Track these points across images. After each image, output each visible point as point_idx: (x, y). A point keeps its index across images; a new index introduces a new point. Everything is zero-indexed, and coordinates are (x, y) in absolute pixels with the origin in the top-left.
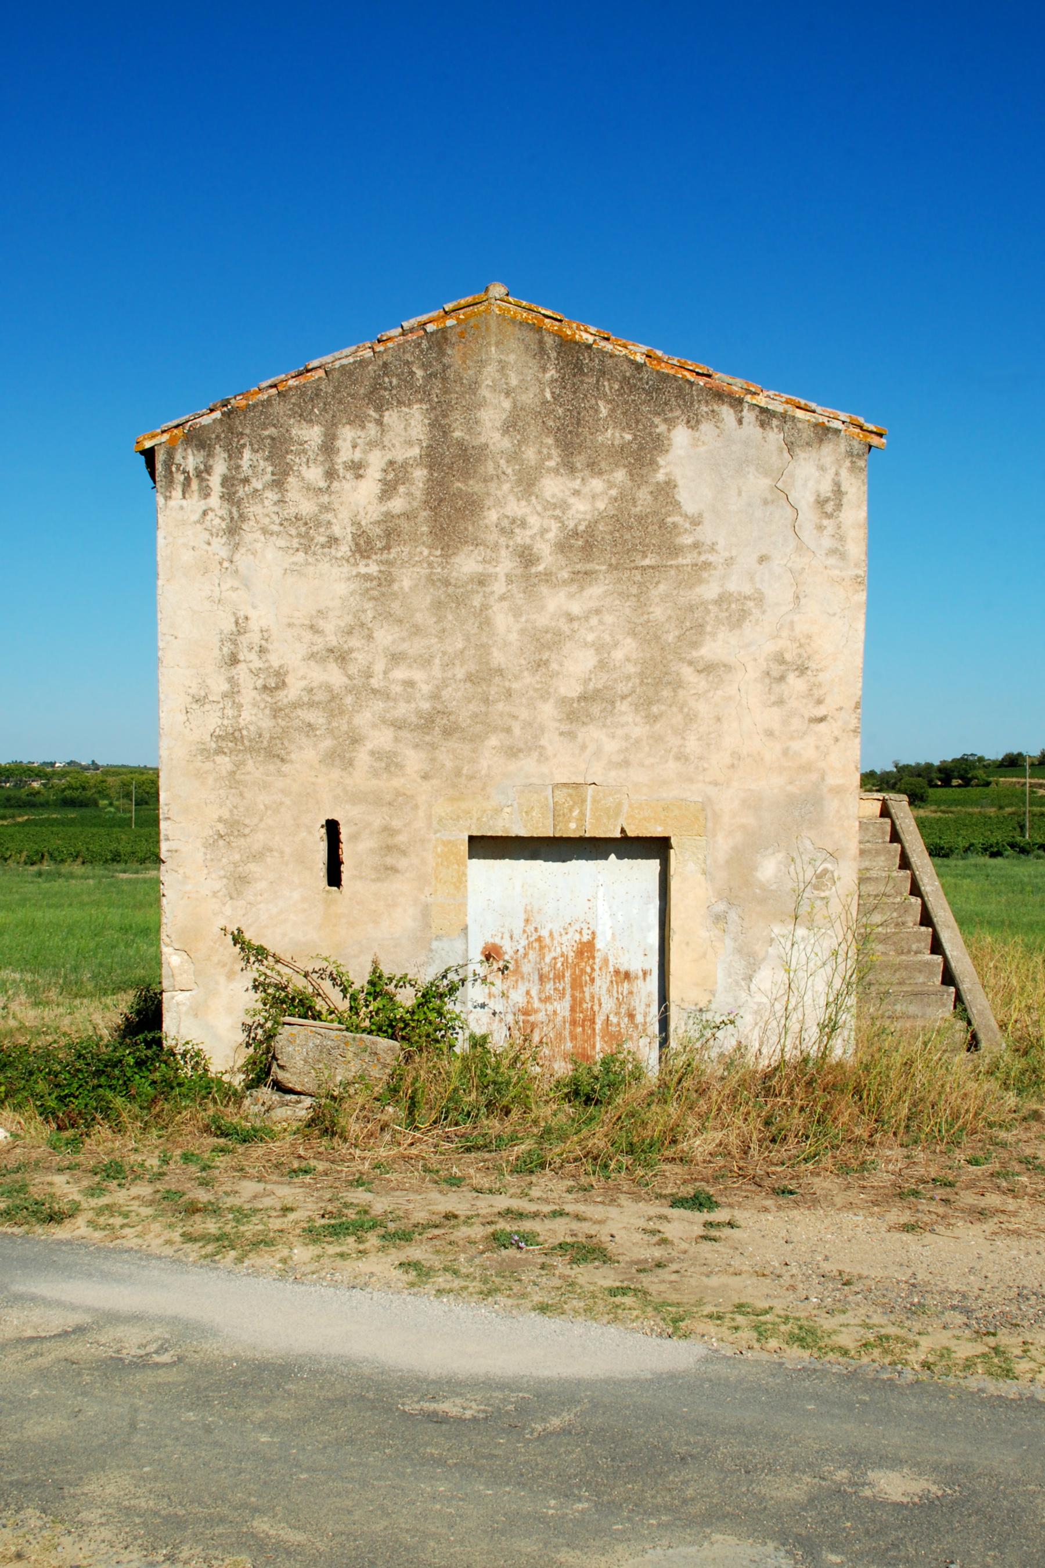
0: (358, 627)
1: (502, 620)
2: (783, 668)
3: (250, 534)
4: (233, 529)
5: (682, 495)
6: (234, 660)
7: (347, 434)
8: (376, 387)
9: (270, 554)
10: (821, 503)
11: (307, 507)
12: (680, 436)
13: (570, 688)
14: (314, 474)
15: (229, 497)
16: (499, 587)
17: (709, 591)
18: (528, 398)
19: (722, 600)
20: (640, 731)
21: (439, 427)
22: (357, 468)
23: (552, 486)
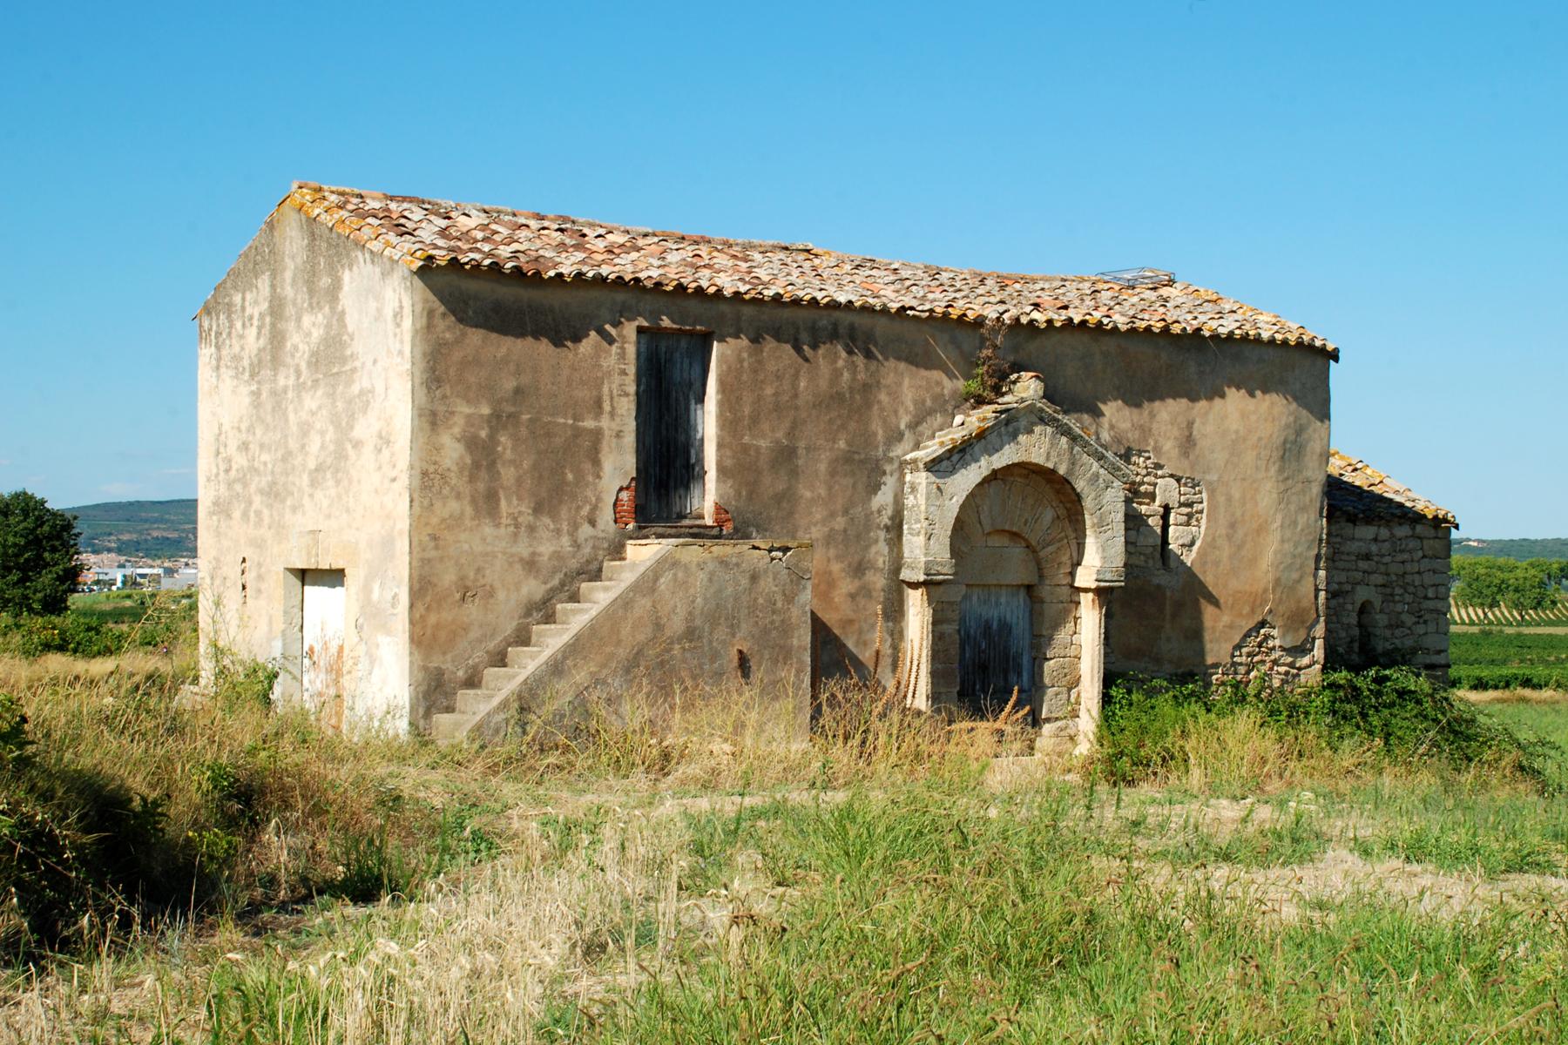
0: (251, 429)
1: (291, 417)
2: (385, 440)
3: (223, 370)
4: (218, 368)
5: (348, 320)
6: (218, 453)
7: (249, 296)
8: (256, 264)
9: (228, 381)
10: (395, 316)
11: (236, 349)
12: (346, 276)
13: (312, 465)
14: (239, 325)
15: (218, 347)
16: (290, 394)
17: (355, 389)
18: (299, 260)
19: (362, 393)
20: (333, 492)
21: (273, 287)
22: (251, 318)
23: (307, 320)
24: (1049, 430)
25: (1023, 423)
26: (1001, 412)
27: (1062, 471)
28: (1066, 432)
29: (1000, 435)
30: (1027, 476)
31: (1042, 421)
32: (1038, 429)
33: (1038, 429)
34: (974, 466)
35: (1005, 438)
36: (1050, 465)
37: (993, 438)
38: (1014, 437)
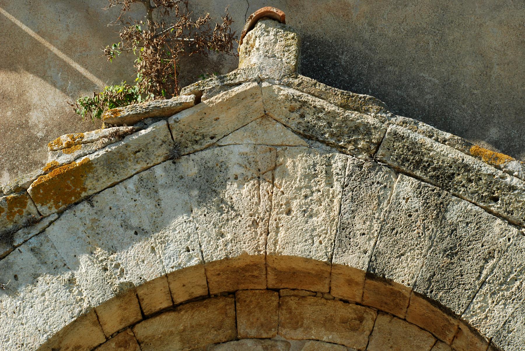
24: (338, 160)
25: (237, 150)
26: (139, 121)
27: (407, 272)
28: (412, 162)
29: (148, 187)
30: (353, 326)
31: (309, 135)
32: (297, 164)
33: (297, 164)
34: (48, 284)
35: (170, 196)
36: (354, 260)
37: (125, 197)
38: (208, 188)
